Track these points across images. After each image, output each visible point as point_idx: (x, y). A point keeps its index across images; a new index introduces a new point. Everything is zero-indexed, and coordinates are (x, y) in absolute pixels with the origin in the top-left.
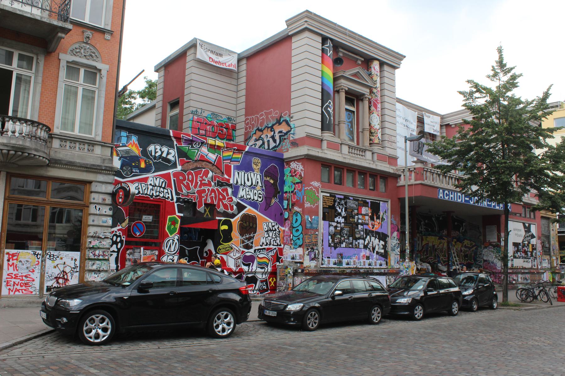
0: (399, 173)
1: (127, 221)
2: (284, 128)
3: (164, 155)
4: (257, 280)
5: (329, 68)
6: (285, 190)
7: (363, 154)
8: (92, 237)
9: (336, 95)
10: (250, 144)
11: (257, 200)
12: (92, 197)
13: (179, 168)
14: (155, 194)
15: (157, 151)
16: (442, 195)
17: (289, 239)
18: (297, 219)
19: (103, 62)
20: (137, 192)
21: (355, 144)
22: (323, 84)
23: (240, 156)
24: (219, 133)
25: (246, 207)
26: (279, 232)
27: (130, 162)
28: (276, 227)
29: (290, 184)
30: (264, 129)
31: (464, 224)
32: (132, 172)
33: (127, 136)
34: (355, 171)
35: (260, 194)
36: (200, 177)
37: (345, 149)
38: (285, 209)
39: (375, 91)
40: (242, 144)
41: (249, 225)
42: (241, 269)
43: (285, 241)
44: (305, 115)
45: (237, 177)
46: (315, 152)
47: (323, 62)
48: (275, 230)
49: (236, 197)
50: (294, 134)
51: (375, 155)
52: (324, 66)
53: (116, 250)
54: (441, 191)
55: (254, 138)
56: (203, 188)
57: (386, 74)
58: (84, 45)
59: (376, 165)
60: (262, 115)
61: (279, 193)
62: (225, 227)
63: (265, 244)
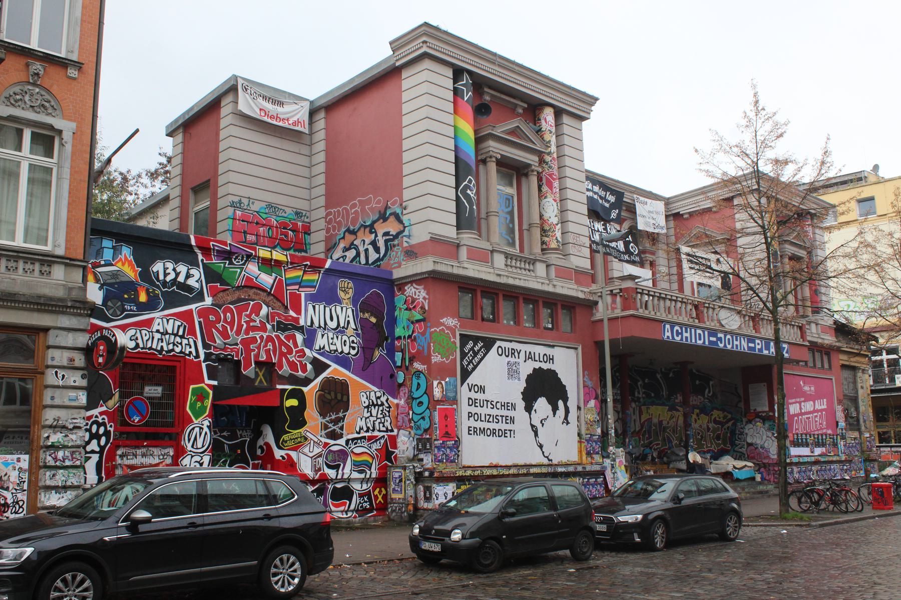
0: (595, 298)
1: (117, 397)
2: (392, 227)
3: (181, 279)
4: (352, 493)
5: (468, 122)
6: (397, 335)
7: (531, 267)
8: (50, 427)
9: (481, 167)
10: (335, 257)
11: (349, 353)
12: (50, 356)
13: (208, 301)
14: (165, 348)
15: (168, 271)
16: (669, 334)
17: (406, 419)
18: (419, 384)
19: (64, 117)
20: (132, 344)
21: (516, 251)
22: (457, 149)
23: (315, 277)
24: (281, 239)
25: (329, 366)
26: (389, 407)
27: (119, 293)
29: (405, 323)
30: (359, 229)
31: (711, 383)
32: (124, 310)
33: (114, 248)
34: (517, 298)
35: (353, 342)
36: (247, 316)
37: (499, 260)
38: (397, 367)
39: (548, 158)
40: (322, 256)
41: (336, 397)
42: (324, 475)
43: (400, 424)
44: (428, 204)
45: (311, 314)
46: (446, 266)
47: (456, 112)
48: (382, 404)
49: (311, 349)
50: (409, 237)
51: (553, 268)
52: (458, 118)
53: (98, 449)
54: (668, 326)
55: (342, 245)
56: (251, 334)
57: (566, 129)
58: (30, 87)
59: (554, 286)
60: (354, 206)
61: (386, 339)
62: (293, 402)
63: (365, 429)
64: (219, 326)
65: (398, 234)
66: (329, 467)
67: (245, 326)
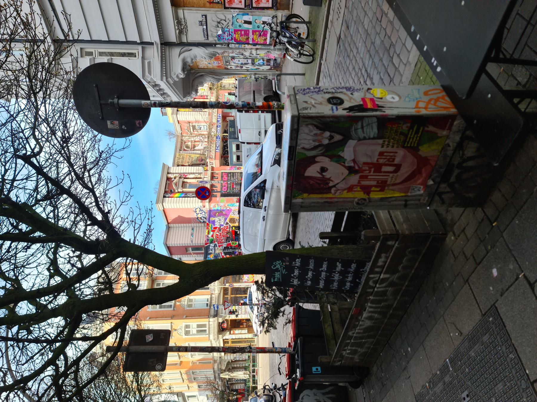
2: (198, 210)
62: (234, 228)
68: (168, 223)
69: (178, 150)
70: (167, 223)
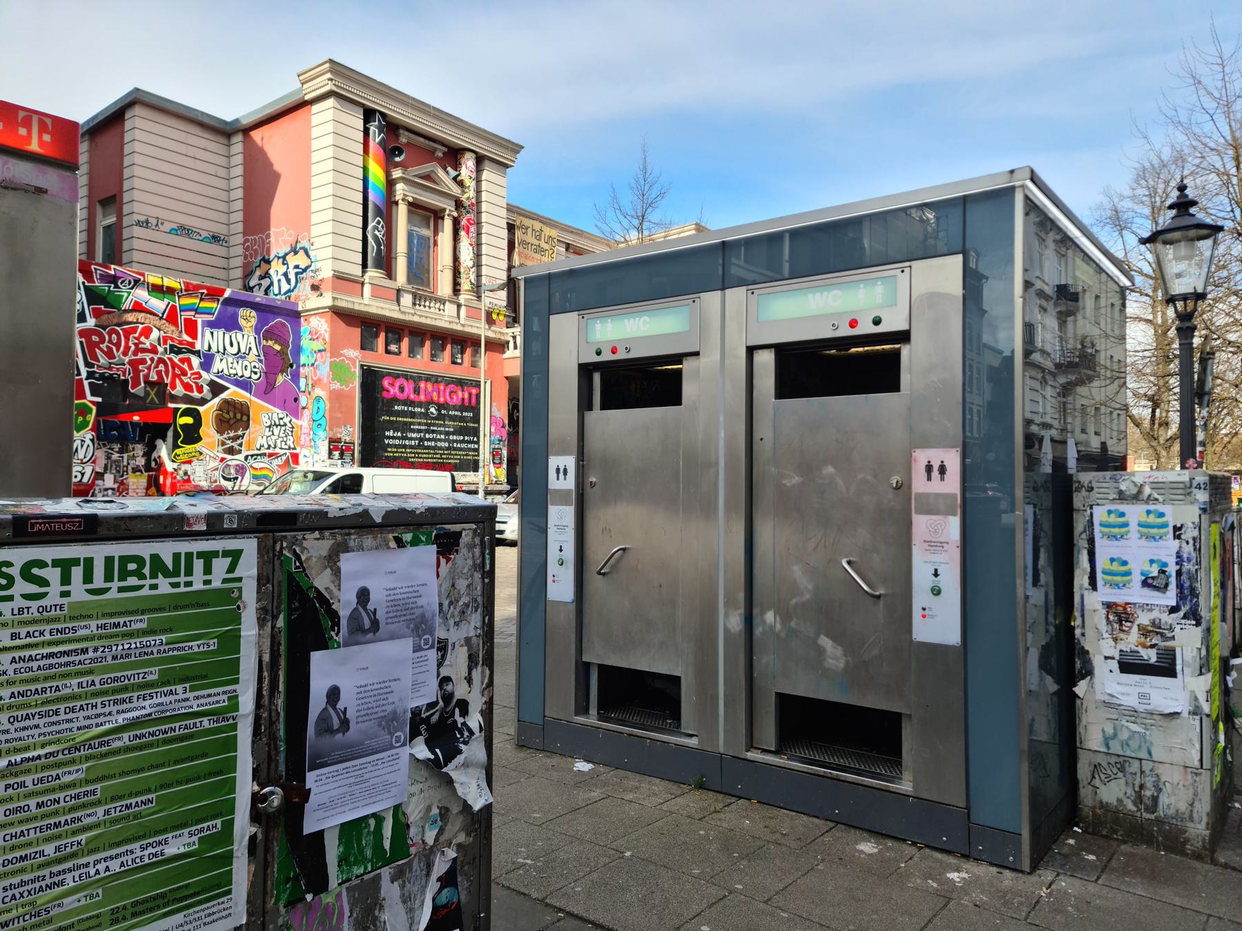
23: (215, 305)
25: (227, 388)
28: (287, 420)
29: (308, 353)
37: (407, 299)
45: (208, 339)
55: (258, 273)
56: (140, 356)
61: (291, 366)
62: (189, 420)
64: (103, 346)
65: (307, 268)
66: (225, 478)
67: (133, 348)
68: (246, 131)
69: (570, 239)
70: (245, 122)
